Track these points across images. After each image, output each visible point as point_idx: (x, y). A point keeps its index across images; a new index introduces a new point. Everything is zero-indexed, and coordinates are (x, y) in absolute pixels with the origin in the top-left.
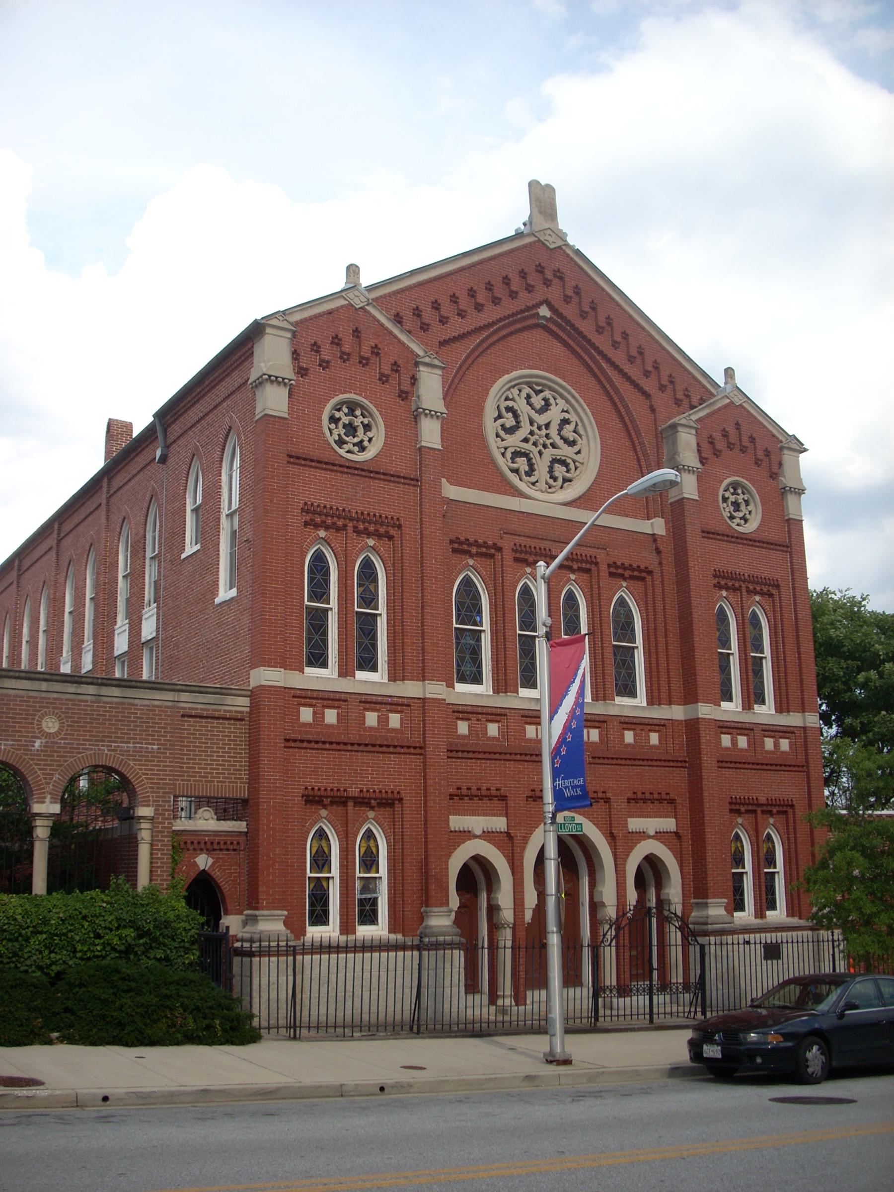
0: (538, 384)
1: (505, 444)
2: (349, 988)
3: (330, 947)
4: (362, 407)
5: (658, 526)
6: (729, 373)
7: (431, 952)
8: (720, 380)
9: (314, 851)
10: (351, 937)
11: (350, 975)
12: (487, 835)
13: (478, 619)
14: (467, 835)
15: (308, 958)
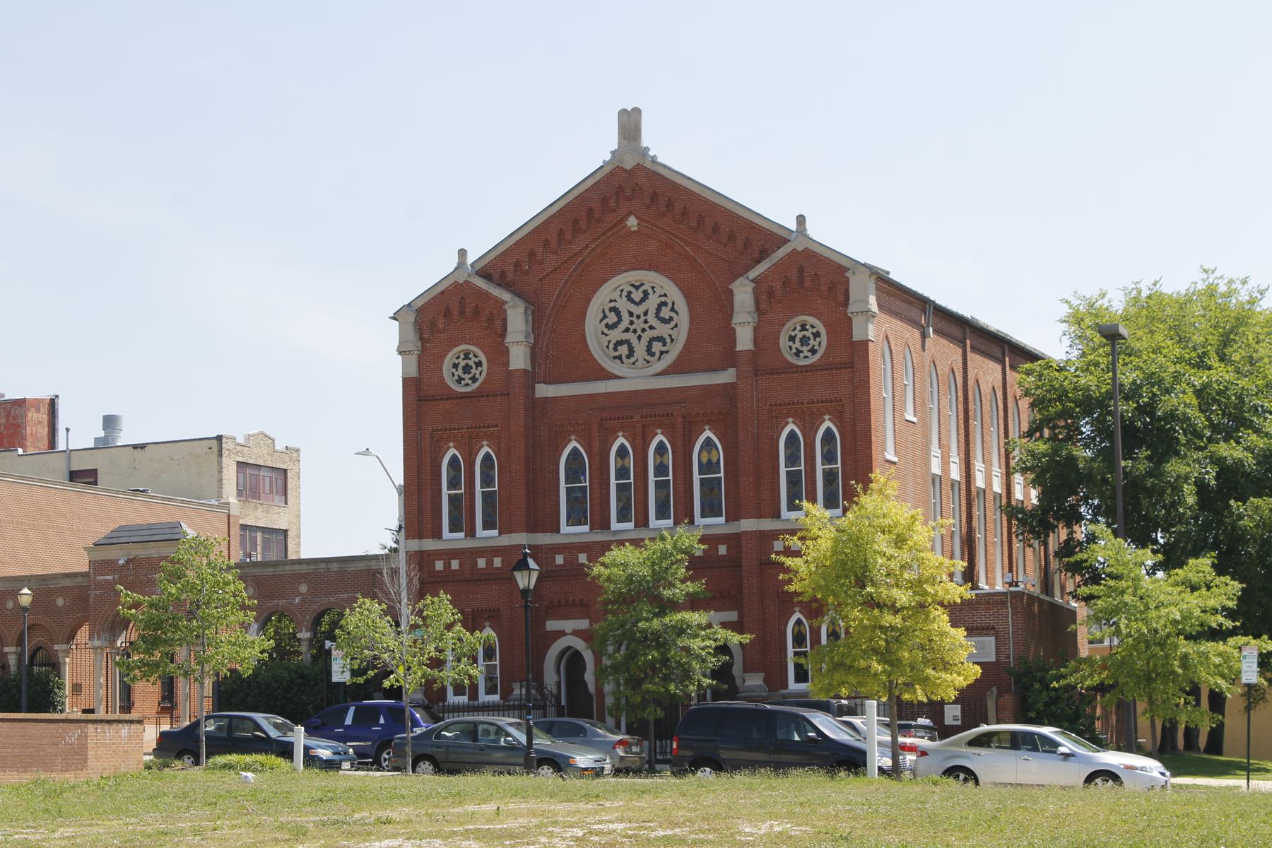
12: (576, 633)
14: (562, 634)
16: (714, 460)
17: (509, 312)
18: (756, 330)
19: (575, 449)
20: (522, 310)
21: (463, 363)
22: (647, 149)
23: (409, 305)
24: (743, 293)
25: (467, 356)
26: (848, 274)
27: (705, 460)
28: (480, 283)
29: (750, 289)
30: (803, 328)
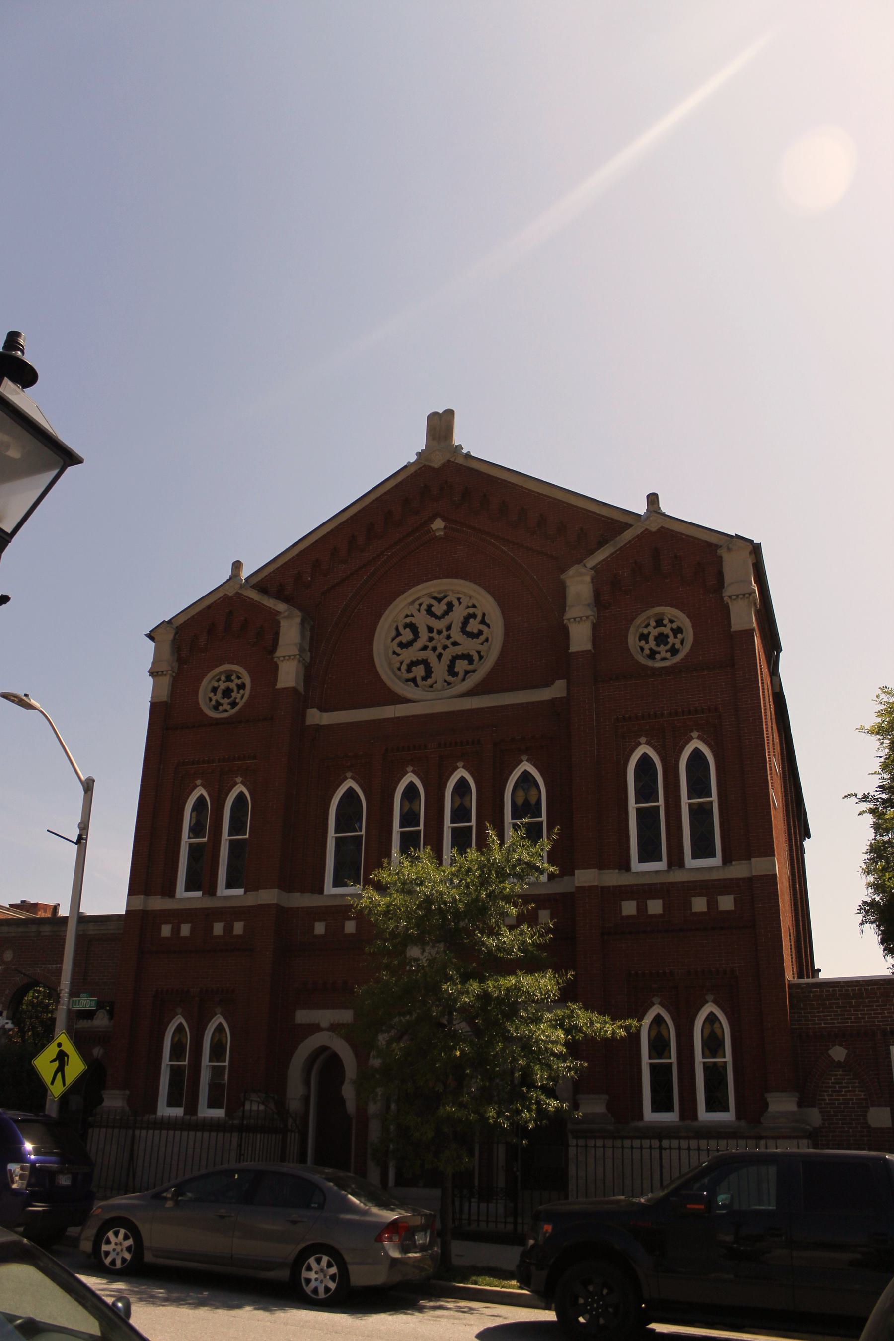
0: (439, 592)
1: (400, 658)
4: (236, 672)
5: (557, 690)
6: (653, 499)
9: (652, 1038)
10: (194, 1118)
14: (315, 1028)
16: (533, 800)
17: (284, 624)
18: (595, 627)
19: (351, 790)
20: (298, 620)
21: (223, 686)
22: (460, 447)
23: (170, 622)
24: (579, 585)
25: (229, 679)
27: (520, 801)
28: (254, 595)
29: (588, 578)
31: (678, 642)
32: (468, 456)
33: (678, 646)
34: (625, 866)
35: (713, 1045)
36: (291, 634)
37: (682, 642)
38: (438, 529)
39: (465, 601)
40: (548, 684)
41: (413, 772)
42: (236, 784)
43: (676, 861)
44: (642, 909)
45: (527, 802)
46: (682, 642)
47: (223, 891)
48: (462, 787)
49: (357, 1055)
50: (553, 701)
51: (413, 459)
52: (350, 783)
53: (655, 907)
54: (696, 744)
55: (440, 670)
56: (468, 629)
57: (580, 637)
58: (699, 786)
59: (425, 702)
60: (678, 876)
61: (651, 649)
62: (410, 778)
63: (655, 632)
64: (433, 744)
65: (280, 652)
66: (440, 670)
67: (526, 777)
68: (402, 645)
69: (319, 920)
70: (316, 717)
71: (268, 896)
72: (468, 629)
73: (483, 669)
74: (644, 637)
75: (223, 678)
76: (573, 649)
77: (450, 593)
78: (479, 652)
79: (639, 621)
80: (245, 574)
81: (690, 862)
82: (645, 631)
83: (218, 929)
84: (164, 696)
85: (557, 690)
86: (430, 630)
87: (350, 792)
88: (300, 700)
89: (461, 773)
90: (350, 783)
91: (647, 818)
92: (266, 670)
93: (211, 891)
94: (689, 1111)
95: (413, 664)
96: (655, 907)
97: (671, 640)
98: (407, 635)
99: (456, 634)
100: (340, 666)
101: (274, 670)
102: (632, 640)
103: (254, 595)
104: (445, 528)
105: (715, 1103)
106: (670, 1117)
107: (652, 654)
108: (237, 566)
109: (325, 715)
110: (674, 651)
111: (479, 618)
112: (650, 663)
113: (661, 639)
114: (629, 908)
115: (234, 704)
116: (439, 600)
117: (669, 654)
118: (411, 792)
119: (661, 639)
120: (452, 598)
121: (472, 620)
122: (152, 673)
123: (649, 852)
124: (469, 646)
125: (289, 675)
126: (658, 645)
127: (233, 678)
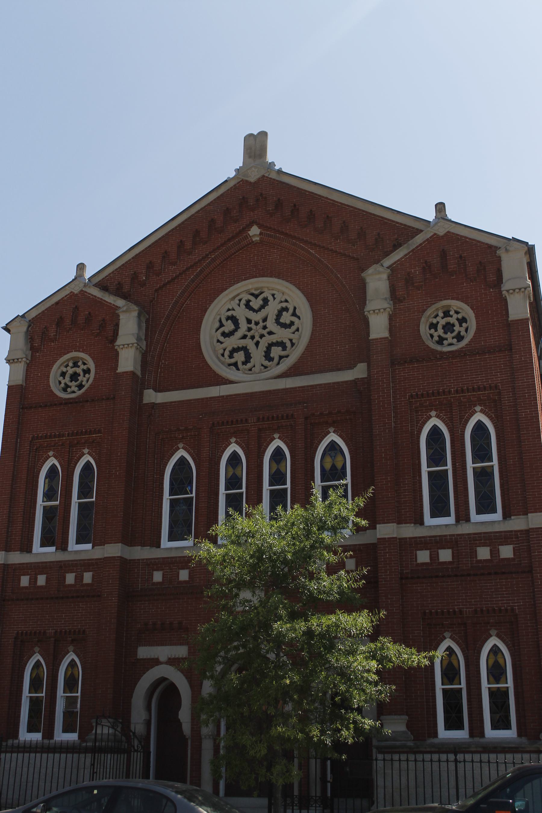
0: (256, 289)
1: (223, 346)
2: (30, 779)
3: (24, 747)
4: (82, 359)
5: (359, 372)
7: (68, 755)
8: (430, 215)
11: (31, 770)
12: (172, 662)
13: (188, 489)
14: (156, 662)
15: (8, 755)
16: (339, 465)
17: (123, 317)
18: (391, 318)
19: (182, 460)
20: (135, 314)
21: (70, 371)
22: (273, 164)
23: (23, 316)
25: (75, 365)
26: (501, 253)
27: (328, 466)
28: (96, 292)
29: (385, 276)
30: (446, 314)
31: (462, 330)
32: (280, 172)
33: (463, 333)
34: (420, 521)
35: (497, 672)
36: (129, 325)
37: (466, 330)
38: (255, 235)
39: (279, 297)
40: (351, 367)
41: (236, 442)
42: (83, 454)
43: (463, 516)
44: (434, 557)
45: (334, 467)
46: (466, 330)
47: (73, 546)
48: (278, 455)
49: (192, 686)
50: (355, 382)
51: (232, 174)
52: (181, 453)
53: (445, 555)
54: (479, 417)
55: (257, 355)
56: (282, 320)
57: (379, 327)
58: (482, 452)
59: (247, 382)
60: (465, 529)
61: (439, 336)
62: (234, 447)
63: (443, 322)
64: (254, 418)
65: (120, 341)
66: (257, 355)
67: (333, 446)
68: (224, 334)
69: (157, 570)
70: (151, 397)
71: (113, 550)
72: (282, 320)
73: (295, 355)
74: (433, 326)
75: (71, 364)
76: (373, 336)
77: (266, 290)
78: (291, 340)
79: (430, 311)
80: (88, 274)
81: (475, 517)
82: (435, 321)
83: (70, 579)
84: (20, 379)
85: (359, 372)
86: (249, 321)
87: (182, 460)
88: (138, 382)
89: (277, 443)
90: (181, 453)
91: (438, 480)
92: (108, 356)
93: (63, 546)
94: (477, 729)
95: (234, 350)
96: (445, 555)
97: (457, 328)
98: (229, 326)
99: (271, 325)
100: (173, 353)
101: (114, 357)
102: (424, 329)
103: (96, 292)
104: (261, 234)
105: (500, 722)
106: (461, 735)
107: (441, 341)
108: (81, 267)
109: (159, 394)
110: (460, 338)
111: (291, 311)
112: (439, 348)
113: (448, 327)
114: (423, 556)
115: (80, 386)
116: (256, 296)
117: (455, 340)
118: (234, 459)
119: (448, 327)
120: (267, 294)
121: (284, 313)
122: (8, 361)
123: (440, 509)
124: (282, 334)
125: (128, 361)
126: (445, 333)
127: (80, 364)
